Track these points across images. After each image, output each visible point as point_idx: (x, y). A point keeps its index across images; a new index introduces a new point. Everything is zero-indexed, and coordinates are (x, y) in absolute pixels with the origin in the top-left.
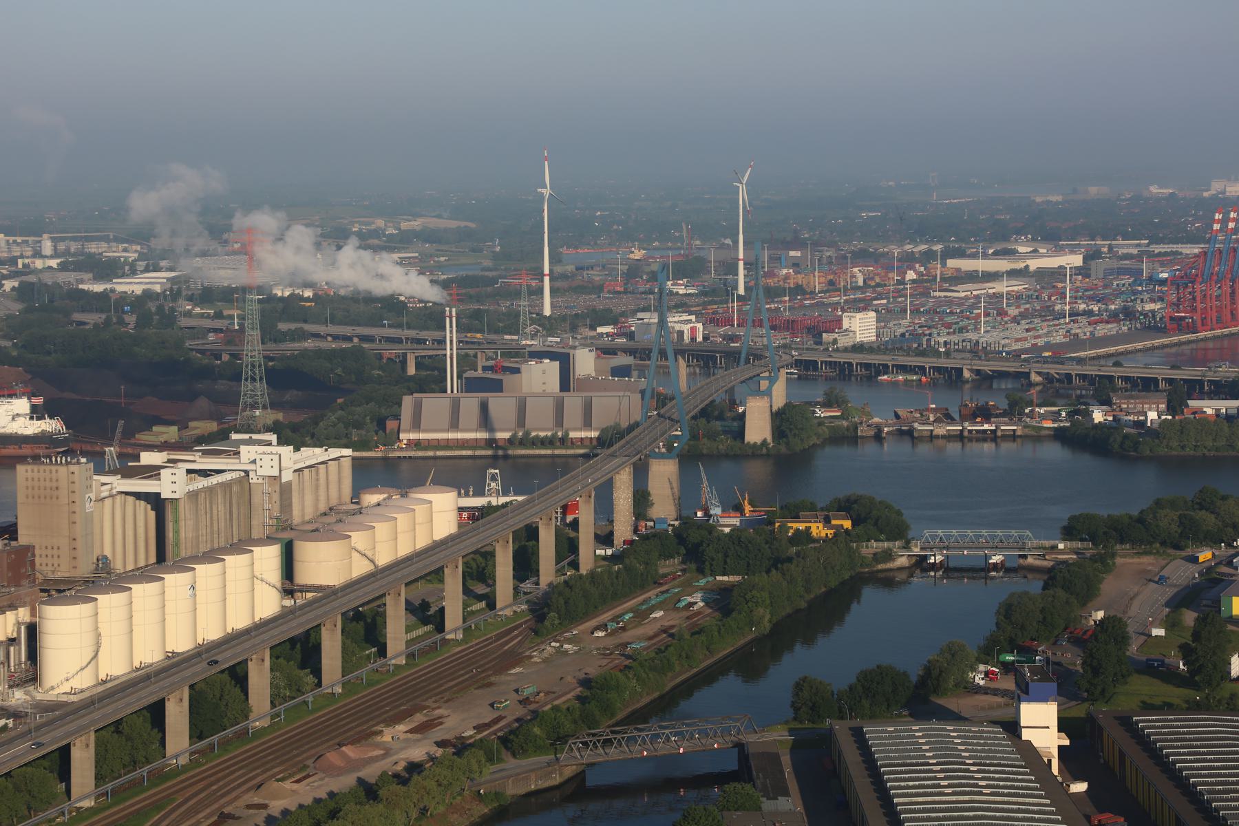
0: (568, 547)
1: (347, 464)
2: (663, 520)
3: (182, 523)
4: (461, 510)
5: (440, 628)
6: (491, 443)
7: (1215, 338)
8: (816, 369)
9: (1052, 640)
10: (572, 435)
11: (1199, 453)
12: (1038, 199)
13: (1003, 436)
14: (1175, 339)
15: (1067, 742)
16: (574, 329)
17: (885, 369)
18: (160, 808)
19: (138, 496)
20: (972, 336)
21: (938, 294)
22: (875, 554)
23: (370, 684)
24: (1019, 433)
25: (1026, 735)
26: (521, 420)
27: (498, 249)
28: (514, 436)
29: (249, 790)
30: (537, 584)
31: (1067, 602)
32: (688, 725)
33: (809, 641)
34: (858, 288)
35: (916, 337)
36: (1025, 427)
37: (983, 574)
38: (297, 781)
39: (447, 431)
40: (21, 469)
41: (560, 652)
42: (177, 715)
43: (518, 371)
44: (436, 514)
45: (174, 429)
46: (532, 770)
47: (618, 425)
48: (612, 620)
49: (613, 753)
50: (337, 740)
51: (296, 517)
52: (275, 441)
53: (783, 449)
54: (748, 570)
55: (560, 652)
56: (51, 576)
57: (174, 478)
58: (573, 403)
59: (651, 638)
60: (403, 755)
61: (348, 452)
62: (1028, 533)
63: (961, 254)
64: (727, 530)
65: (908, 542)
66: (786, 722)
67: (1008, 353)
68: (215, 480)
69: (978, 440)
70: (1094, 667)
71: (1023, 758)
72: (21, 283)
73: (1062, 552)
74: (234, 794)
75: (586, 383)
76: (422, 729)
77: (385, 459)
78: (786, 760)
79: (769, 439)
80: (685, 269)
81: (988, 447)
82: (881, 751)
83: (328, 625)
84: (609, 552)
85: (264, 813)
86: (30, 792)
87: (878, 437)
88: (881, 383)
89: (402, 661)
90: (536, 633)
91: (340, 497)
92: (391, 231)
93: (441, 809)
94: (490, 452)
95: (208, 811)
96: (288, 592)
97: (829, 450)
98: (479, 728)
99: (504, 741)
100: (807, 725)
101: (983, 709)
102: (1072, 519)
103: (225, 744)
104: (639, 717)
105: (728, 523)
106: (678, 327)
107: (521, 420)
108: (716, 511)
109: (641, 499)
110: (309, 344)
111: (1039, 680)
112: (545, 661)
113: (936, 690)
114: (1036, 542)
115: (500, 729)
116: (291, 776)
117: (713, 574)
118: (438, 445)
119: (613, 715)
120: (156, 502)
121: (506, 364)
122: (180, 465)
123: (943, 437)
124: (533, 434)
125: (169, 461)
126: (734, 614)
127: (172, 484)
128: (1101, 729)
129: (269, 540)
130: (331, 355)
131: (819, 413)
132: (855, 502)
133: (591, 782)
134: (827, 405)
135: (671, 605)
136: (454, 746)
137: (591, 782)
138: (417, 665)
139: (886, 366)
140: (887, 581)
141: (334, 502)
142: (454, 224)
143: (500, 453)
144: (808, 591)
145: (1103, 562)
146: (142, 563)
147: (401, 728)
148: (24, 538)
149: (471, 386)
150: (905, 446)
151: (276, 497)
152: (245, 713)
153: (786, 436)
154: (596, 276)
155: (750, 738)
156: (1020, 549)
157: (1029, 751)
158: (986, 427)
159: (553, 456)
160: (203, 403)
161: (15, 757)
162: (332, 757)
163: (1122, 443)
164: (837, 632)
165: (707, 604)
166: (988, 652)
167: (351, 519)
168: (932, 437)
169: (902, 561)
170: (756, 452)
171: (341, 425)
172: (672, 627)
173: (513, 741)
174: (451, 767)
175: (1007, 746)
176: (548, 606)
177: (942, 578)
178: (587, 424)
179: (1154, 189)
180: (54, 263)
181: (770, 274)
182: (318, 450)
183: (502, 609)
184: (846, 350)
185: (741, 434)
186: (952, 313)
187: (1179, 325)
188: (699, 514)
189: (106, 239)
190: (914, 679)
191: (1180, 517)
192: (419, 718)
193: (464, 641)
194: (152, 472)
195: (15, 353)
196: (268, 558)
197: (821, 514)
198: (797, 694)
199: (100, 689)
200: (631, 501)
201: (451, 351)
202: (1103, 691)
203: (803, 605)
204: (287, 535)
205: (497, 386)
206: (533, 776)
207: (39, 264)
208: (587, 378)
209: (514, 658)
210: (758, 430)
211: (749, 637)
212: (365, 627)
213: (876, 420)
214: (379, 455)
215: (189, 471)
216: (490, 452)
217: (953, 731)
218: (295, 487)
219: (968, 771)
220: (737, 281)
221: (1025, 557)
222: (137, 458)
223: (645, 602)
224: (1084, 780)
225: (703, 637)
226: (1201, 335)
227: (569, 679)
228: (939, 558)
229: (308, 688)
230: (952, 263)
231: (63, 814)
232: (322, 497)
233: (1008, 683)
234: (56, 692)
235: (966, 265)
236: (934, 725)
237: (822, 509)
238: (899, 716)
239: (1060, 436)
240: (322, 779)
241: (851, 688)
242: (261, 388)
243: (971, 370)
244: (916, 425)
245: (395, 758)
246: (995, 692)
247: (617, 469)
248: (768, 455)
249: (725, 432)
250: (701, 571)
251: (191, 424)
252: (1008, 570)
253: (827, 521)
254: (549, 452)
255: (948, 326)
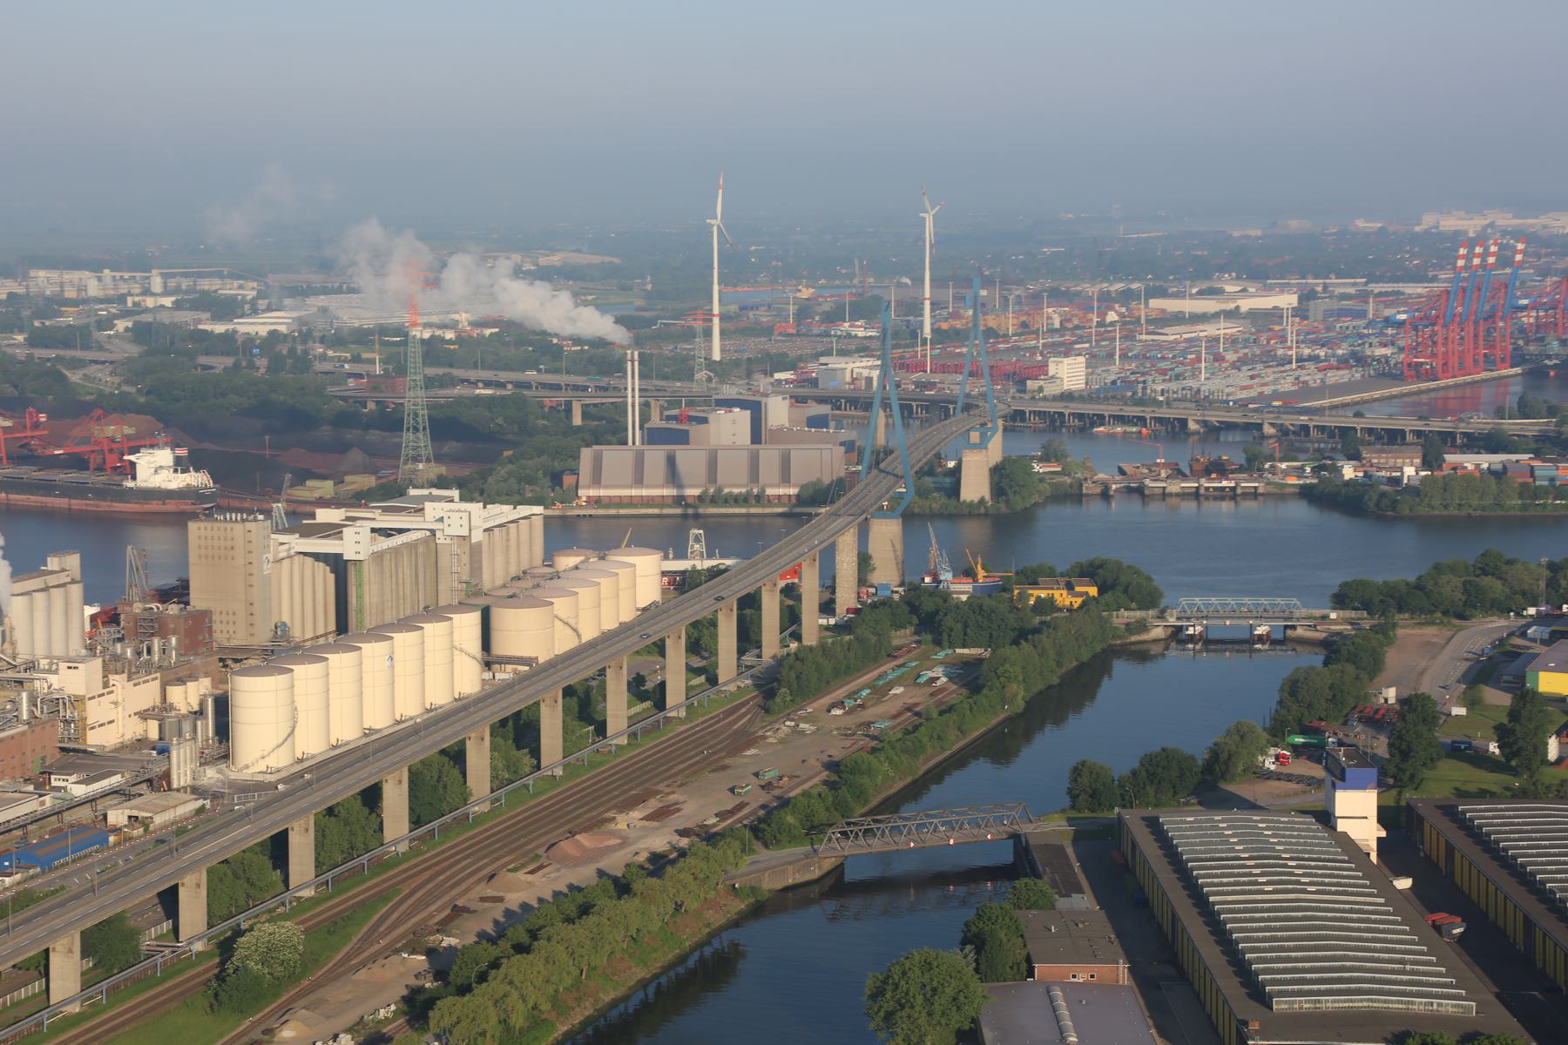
0: (791, 617)
1: (538, 523)
2: (886, 587)
3: (366, 588)
4: (664, 574)
5: (660, 704)
6: (679, 500)
7: (1457, 386)
8: (1023, 420)
9: (1341, 720)
10: (770, 491)
11: (1464, 513)
12: (1236, 234)
13: (1244, 494)
14: (1414, 387)
15: (1383, 834)
16: (749, 375)
17: (1101, 419)
18: (387, 900)
19: (317, 557)
20: (1190, 383)
21: (1144, 337)
22: (1127, 625)
23: (592, 765)
24: (1261, 491)
25: (1342, 826)
26: (712, 475)
27: (649, 287)
28: (705, 492)
29: (479, 881)
30: (760, 656)
31: (1357, 678)
32: (958, 814)
33: (1059, 720)
34: (1052, 331)
35: (1128, 384)
36: (1268, 484)
37: (1245, 647)
38: (531, 872)
40: (193, 526)
41: (796, 731)
42: (396, 799)
43: (704, 421)
44: (640, 578)
45: (330, 483)
46: (790, 863)
47: (819, 481)
48: (849, 696)
49: (877, 845)
50: (567, 827)
51: (487, 584)
52: (457, 498)
53: (1003, 508)
54: (990, 642)
55: (796, 731)
56: (226, 644)
57: (358, 538)
58: (769, 456)
59: (894, 717)
60: (641, 845)
61: (539, 509)
62: (1295, 601)
63: (1162, 293)
64: (964, 598)
65: (1163, 611)
66: (1063, 811)
67: (1235, 402)
68: (398, 540)
69: (1215, 498)
70: (1402, 750)
71: (1345, 852)
72: (136, 323)
73: (1334, 622)
74: (464, 886)
75: (778, 435)
76: (659, 815)
77: (563, 518)
78: (1070, 851)
79: (988, 497)
80: (864, 309)
81: (1226, 506)
82: (1186, 844)
83: (548, 701)
84: (832, 621)
85: (501, 907)
86: (248, 880)
87: (1105, 495)
88: (1097, 435)
89: (624, 741)
90: (767, 711)
91: (531, 559)
92: (528, 267)
93: (695, 905)
94: (679, 511)
95: (439, 903)
96: (488, 665)
97: (1052, 510)
98: (722, 815)
99: (755, 830)
100: (1087, 814)
101: (1279, 796)
102: (1344, 585)
103: (445, 829)
104: (892, 805)
105: (962, 590)
106: (865, 373)
107: (712, 475)
108: (946, 576)
109: (864, 562)
110: (458, 391)
111: (1356, 766)
112: (781, 741)
113: (1224, 775)
114: (1304, 612)
115: (746, 817)
116: (523, 866)
117: (952, 646)
118: (620, 502)
119: (866, 801)
120: (338, 565)
121: (693, 414)
122: (359, 523)
123: (1177, 495)
124: (726, 491)
125: (348, 519)
126: (985, 691)
127: (355, 543)
128: (1421, 820)
129: (462, 607)
130: (490, 402)
131: (1037, 468)
132: (1101, 566)
133: (849, 876)
134: (1045, 459)
135: (913, 680)
136: (698, 835)
137: (849, 876)
138: (639, 745)
139: (1101, 417)
140: (1141, 655)
141: (525, 566)
142: (596, 259)
143: (690, 511)
144: (1059, 664)
145: (1384, 631)
146: (321, 631)
147: (636, 814)
148: (197, 601)
149: (653, 437)
150: (1135, 505)
151: (465, 559)
152: (465, 798)
153: (1005, 494)
154: (764, 317)
155: (1026, 828)
156: (1286, 619)
157: (1345, 842)
158: (1225, 483)
159: (749, 515)
160: (356, 455)
161: (235, 842)
162: (566, 846)
163: (1377, 505)
164: (1089, 712)
165: (951, 679)
166: (1277, 732)
167: (549, 584)
168: (1164, 495)
169: (1158, 632)
170: (973, 512)
171: (513, 480)
172: (917, 704)
173: (763, 829)
174: (707, 859)
175: (1323, 838)
176: (778, 680)
177: (1200, 651)
178: (785, 479)
179: (1361, 224)
180: (168, 301)
181: (955, 315)
182: (507, 508)
183: (726, 684)
184: (1055, 398)
185: (955, 491)
186: (1163, 358)
187: (1418, 373)
188: (927, 580)
189: (220, 275)
190: (1200, 763)
191: (1464, 583)
192: (653, 804)
193: (688, 719)
194: (333, 531)
195: (142, 400)
196: (467, 625)
197: (1063, 580)
198: (1075, 780)
199: (298, 768)
200: (855, 565)
201: (633, 399)
202: (1412, 777)
203: (1055, 681)
204: (482, 601)
205: (682, 438)
206: (790, 868)
207: (150, 302)
208: (781, 429)
209: (745, 740)
210: (975, 487)
211: (1002, 716)
212: (584, 705)
213: (1101, 476)
214: (557, 513)
215: (373, 530)
216: (679, 511)
217: (1262, 821)
218: (485, 548)
219: (1286, 866)
220: (921, 324)
221: (1294, 627)
222: (313, 516)
223: (880, 677)
224: (1407, 876)
225: (954, 717)
226: (1442, 383)
227: (812, 761)
228: (1199, 629)
229: (527, 770)
230: (1155, 303)
231: (283, 904)
232: (513, 560)
233: (1317, 771)
234: (251, 770)
235: (1171, 305)
236: (1236, 814)
237: (1062, 575)
238: (1187, 804)
239: (1306, 493)
240: (558, 870)
241: (1134, 773)
242: (423, 441)
243: (1197, 422)
244: (1147, 481)
245: (634, 848)
246: (1289, 778)
247: (840, 531)
248: (986, 515)
249: (937, 489)
250: (938, 643)
251: (348, 478)
252: (1274, 642)
253: (1070, 587)
254: (743, 511)
255: (1163, 372)
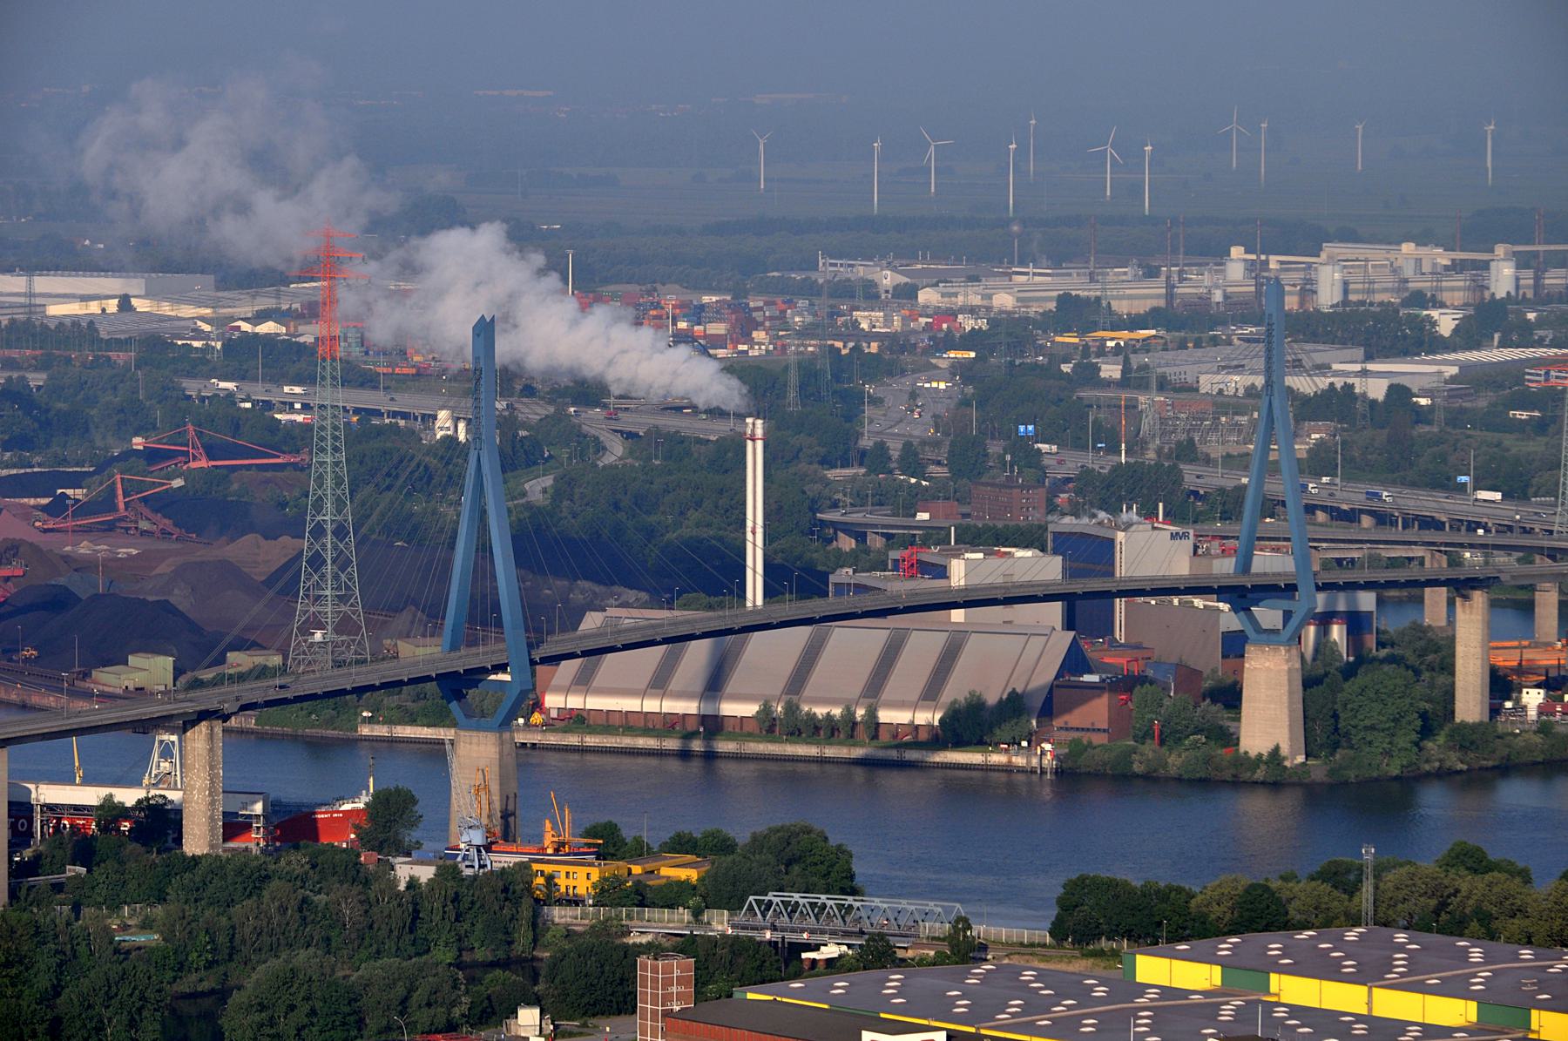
39: (643, 694)
53: (1319, 771)
143: (697, 745)
170: (1271, 776)
178: (930, 695)
254: (813, 751)
